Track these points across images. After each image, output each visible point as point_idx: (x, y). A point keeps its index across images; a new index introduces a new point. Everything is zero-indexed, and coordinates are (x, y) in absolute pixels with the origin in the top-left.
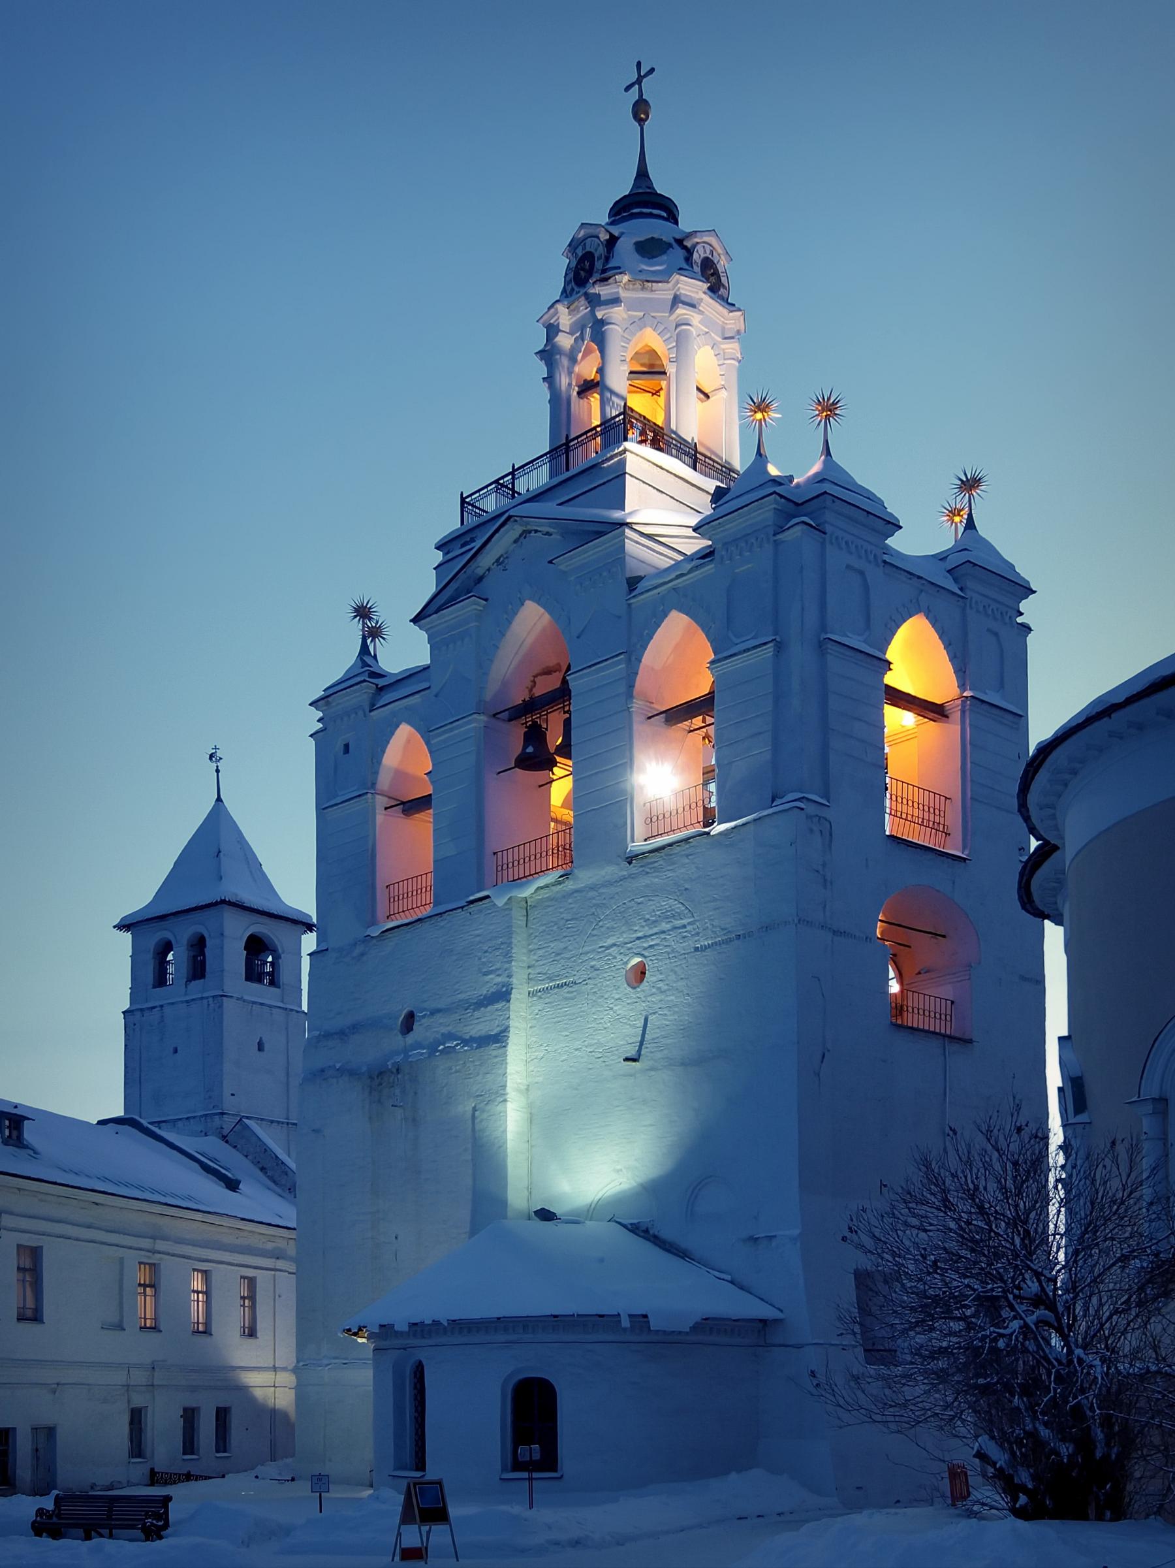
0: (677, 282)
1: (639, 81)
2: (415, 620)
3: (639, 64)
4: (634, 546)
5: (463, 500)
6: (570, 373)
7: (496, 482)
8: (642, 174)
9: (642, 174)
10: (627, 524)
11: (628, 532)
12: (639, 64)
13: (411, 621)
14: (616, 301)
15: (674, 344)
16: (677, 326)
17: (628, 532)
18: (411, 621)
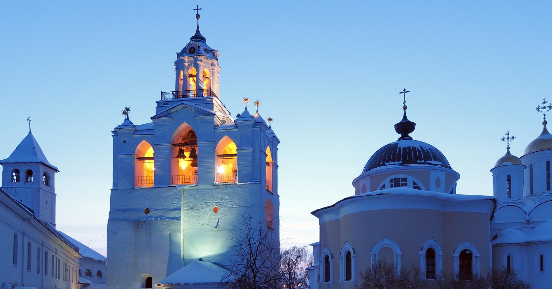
0: (214, 61)
1: (197, 9)
2: (151, 118)
3: (197, 6)
4: (216, 119)
5: (162, 93)
6: (187, 72)
7: (172, 92)
8: (198, 31)
9: (198, 31)
10: (216, 115)
11: (216, 116)
12: (197, 6)
13: (150, 118)
14: (201, 61)
15: (211, 73)
16: (212, 70)
17: (216, 116)
18: (150, 118)
